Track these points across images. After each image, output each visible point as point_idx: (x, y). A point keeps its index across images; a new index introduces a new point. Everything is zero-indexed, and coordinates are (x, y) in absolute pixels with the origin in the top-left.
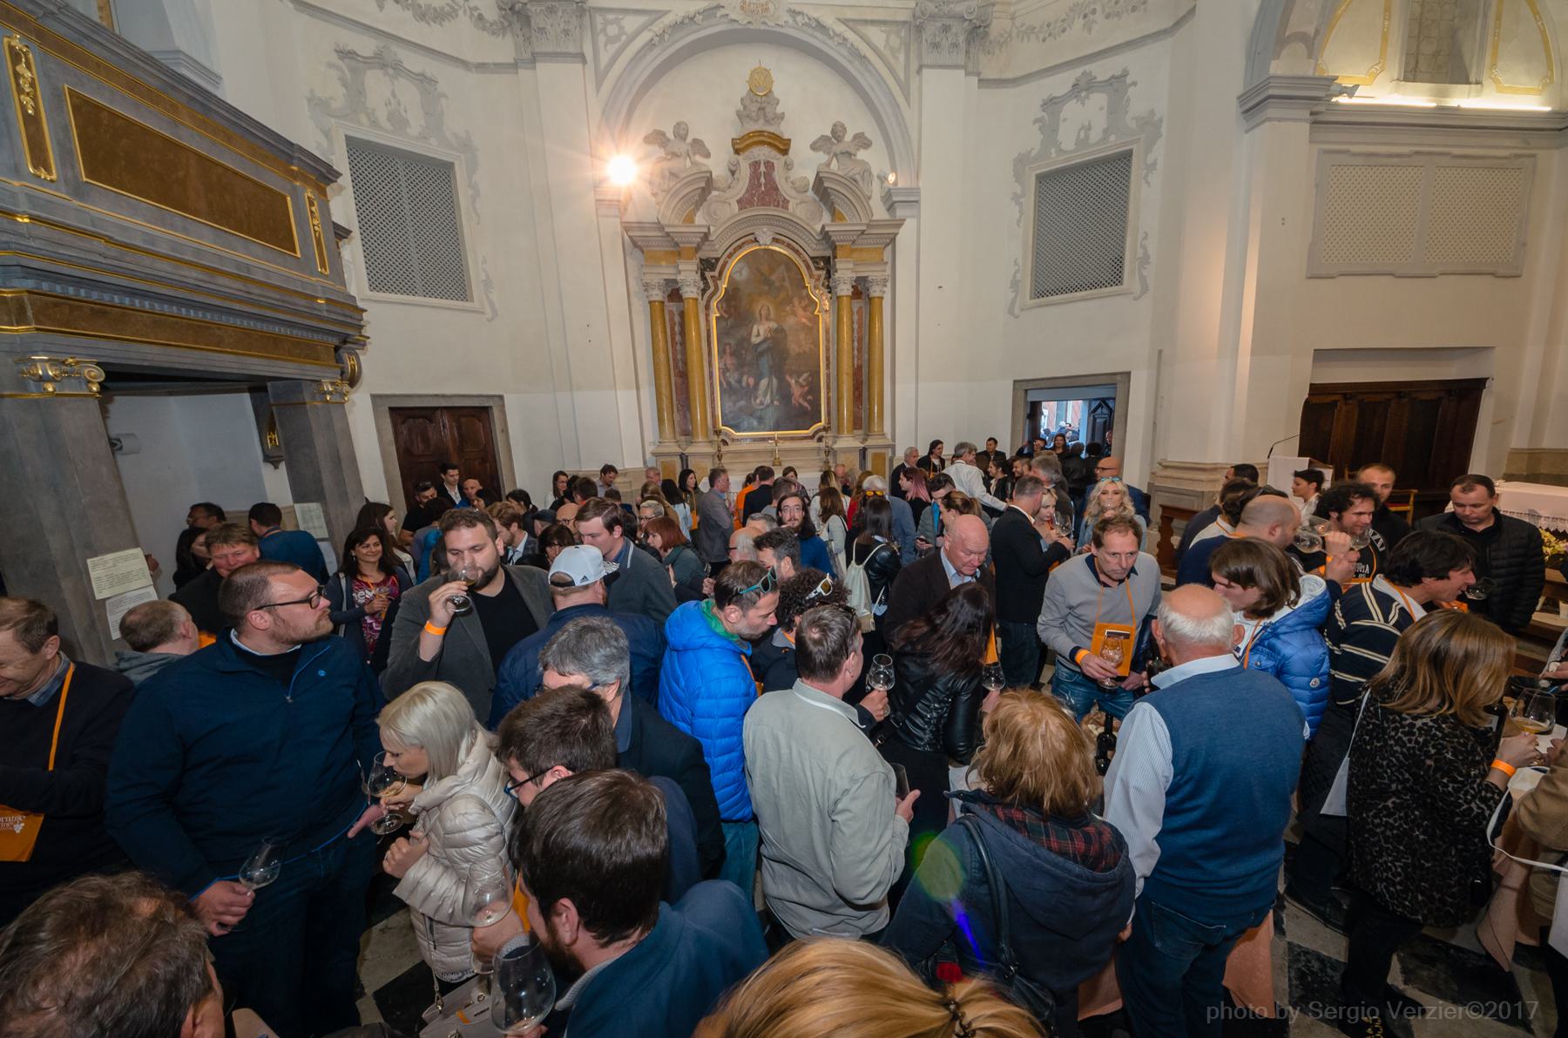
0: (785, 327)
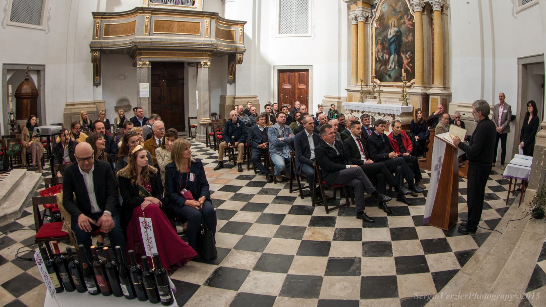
0: (401, 29)
